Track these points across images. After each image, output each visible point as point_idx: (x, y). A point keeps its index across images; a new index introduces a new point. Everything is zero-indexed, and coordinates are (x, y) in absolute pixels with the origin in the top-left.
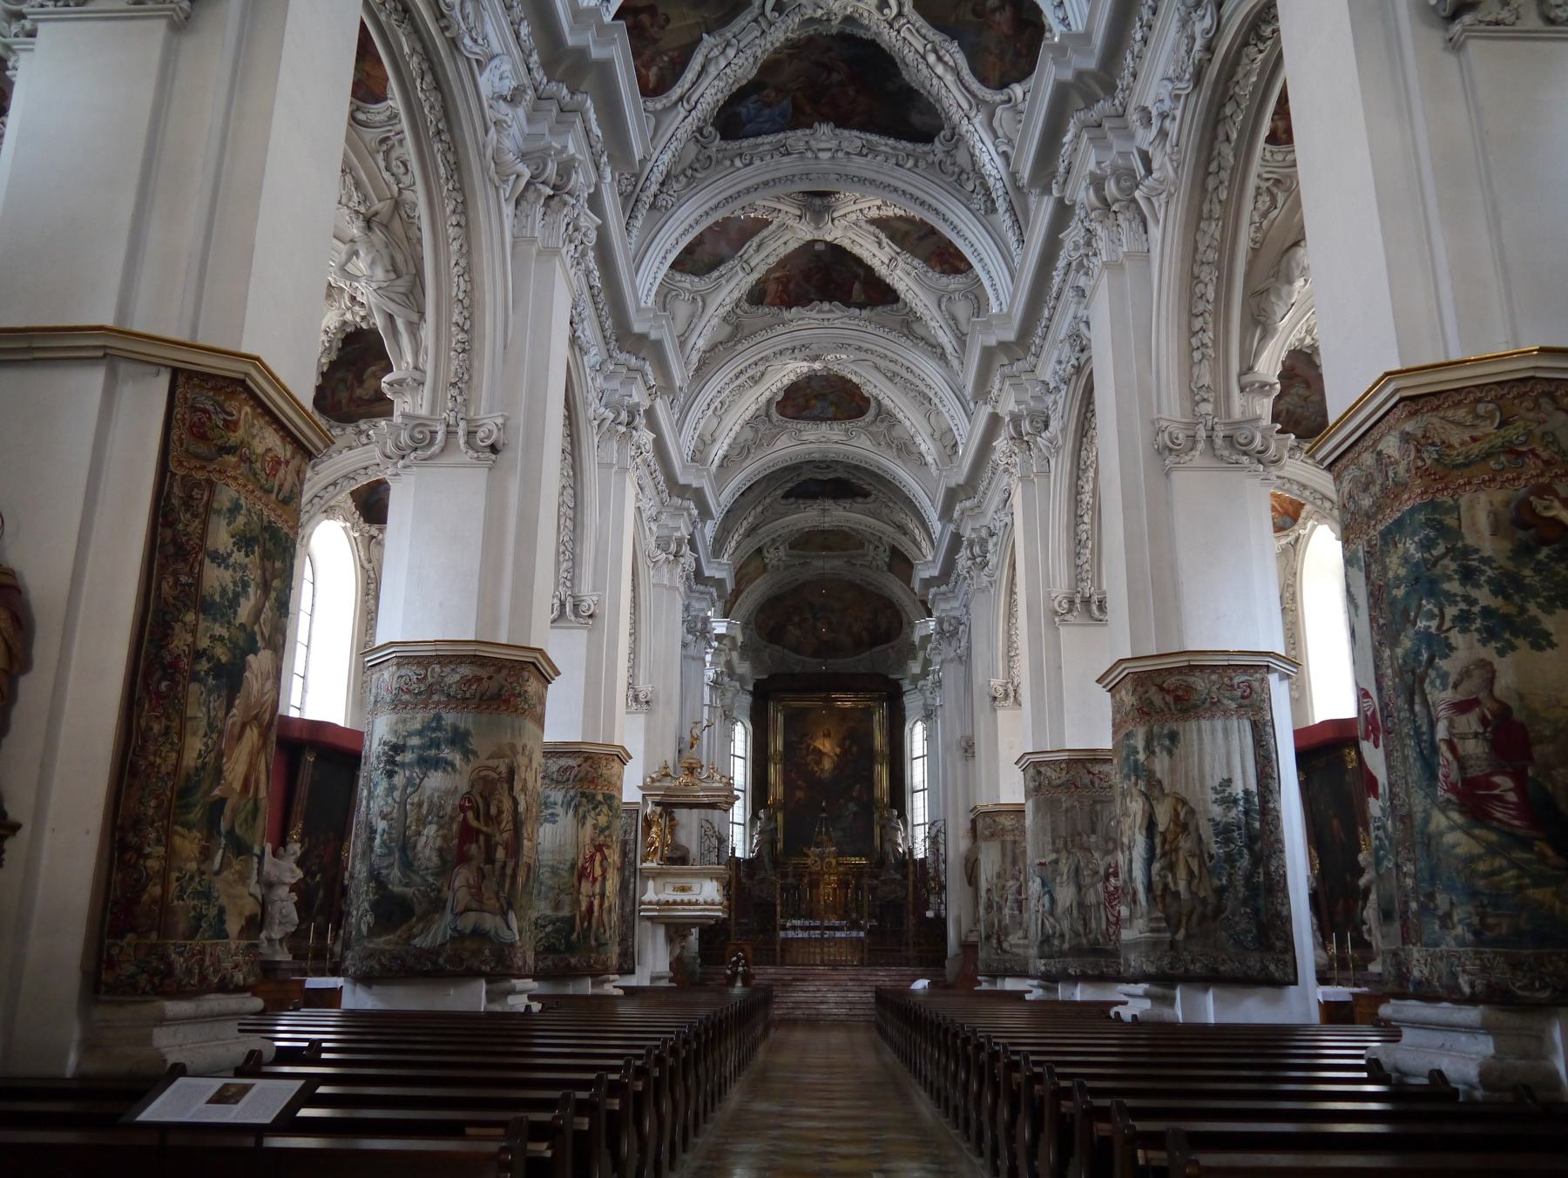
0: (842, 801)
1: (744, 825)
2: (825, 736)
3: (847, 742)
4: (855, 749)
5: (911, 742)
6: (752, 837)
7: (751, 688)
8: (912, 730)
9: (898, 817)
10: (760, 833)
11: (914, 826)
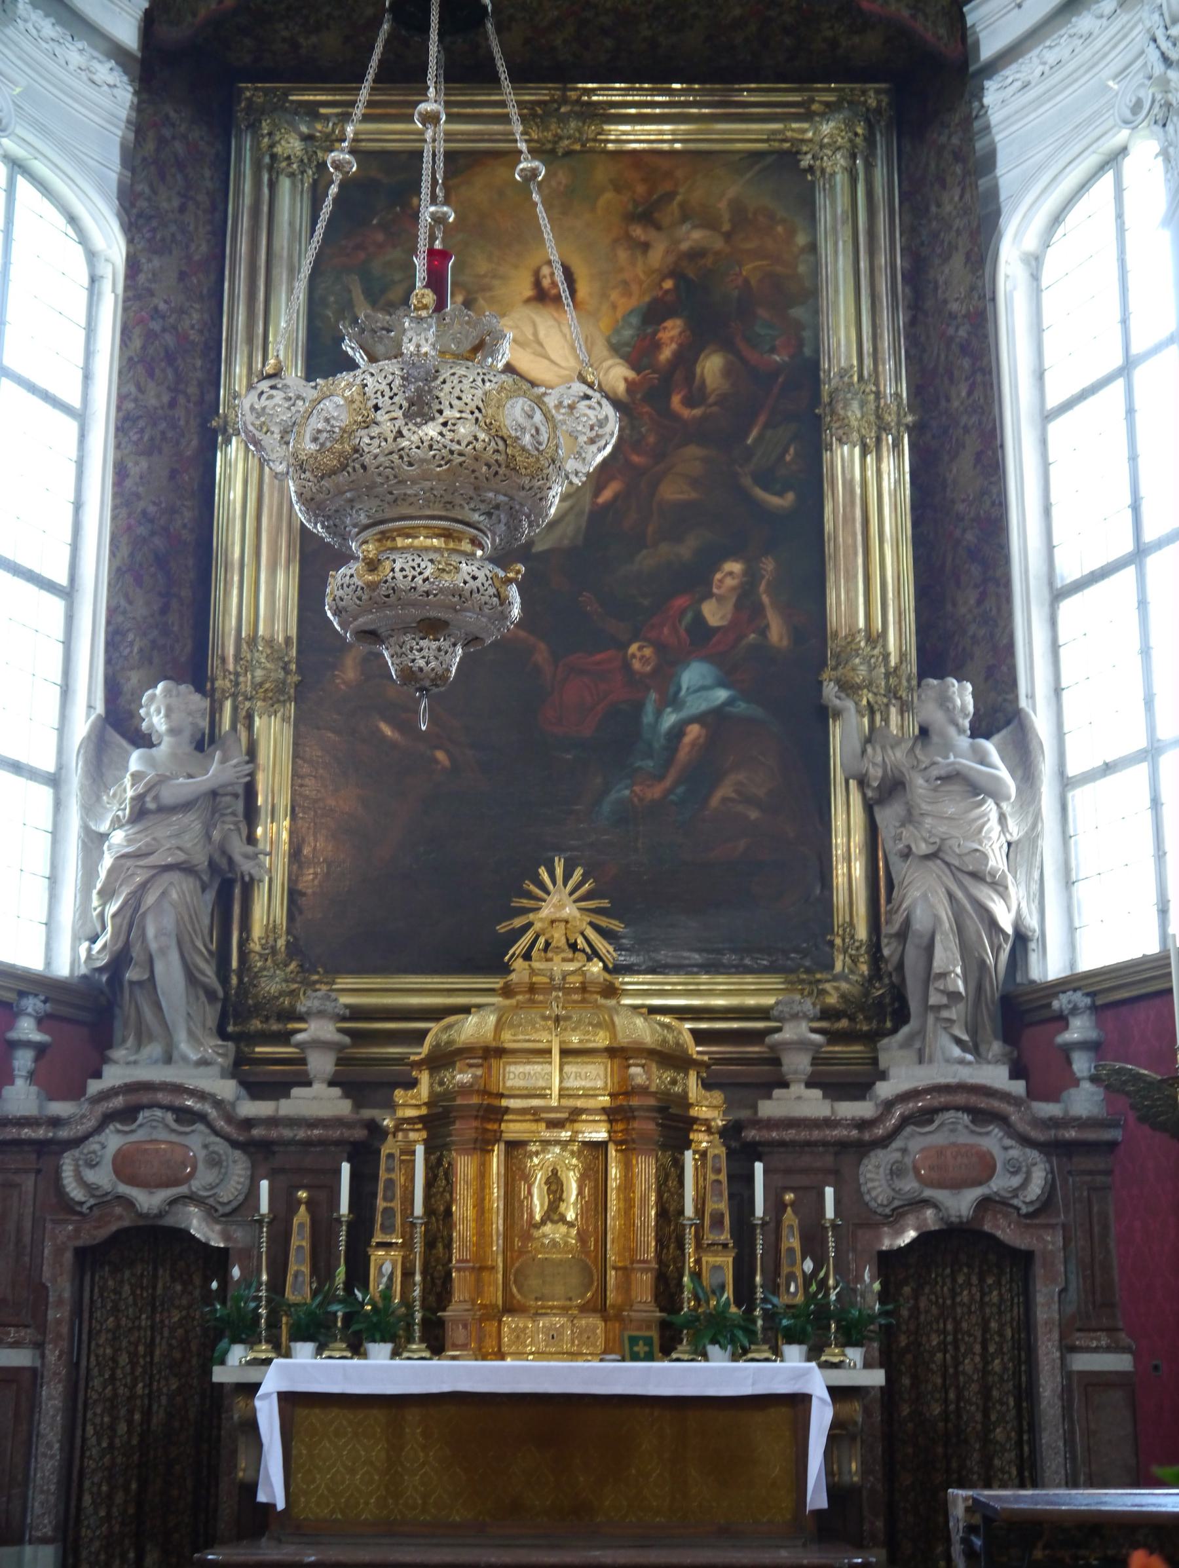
0: (640, 654)
1: (55, 781)
2: (543, 296)
3: (672, 331)
4: (712, 366)
5: (1038, 330)
6: (94, 841)
7: (127, 34)
8: (1034, 263)
9: (982, 727)
10: (140, 813)
11: (1066, 783)
